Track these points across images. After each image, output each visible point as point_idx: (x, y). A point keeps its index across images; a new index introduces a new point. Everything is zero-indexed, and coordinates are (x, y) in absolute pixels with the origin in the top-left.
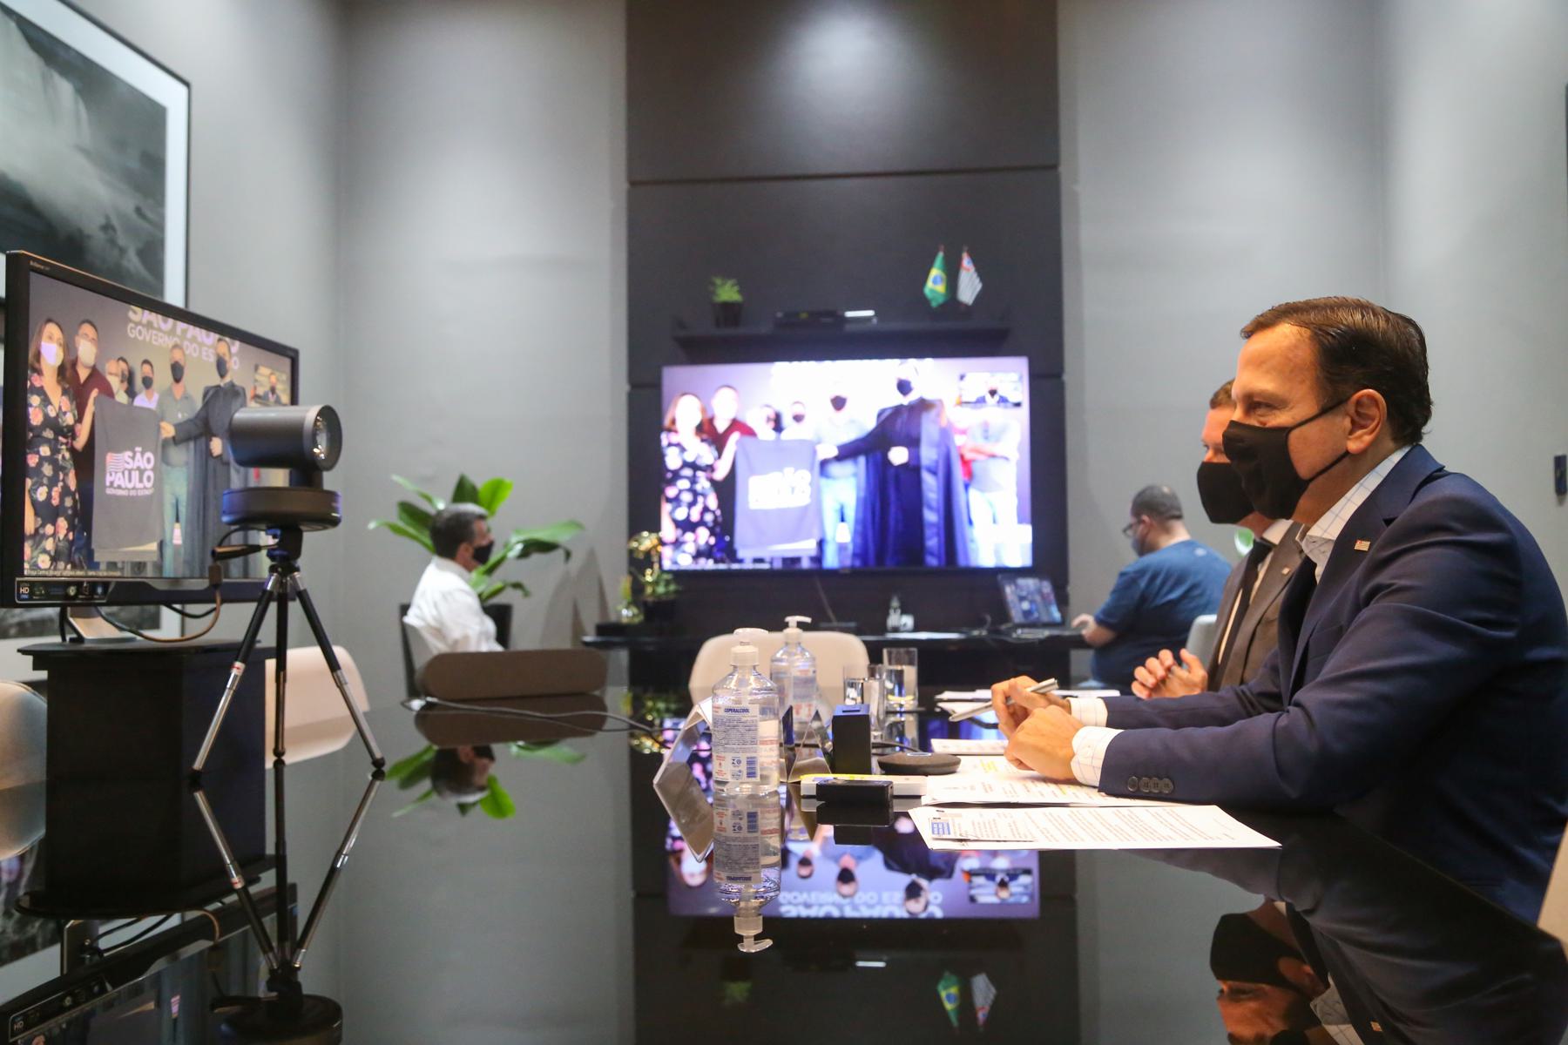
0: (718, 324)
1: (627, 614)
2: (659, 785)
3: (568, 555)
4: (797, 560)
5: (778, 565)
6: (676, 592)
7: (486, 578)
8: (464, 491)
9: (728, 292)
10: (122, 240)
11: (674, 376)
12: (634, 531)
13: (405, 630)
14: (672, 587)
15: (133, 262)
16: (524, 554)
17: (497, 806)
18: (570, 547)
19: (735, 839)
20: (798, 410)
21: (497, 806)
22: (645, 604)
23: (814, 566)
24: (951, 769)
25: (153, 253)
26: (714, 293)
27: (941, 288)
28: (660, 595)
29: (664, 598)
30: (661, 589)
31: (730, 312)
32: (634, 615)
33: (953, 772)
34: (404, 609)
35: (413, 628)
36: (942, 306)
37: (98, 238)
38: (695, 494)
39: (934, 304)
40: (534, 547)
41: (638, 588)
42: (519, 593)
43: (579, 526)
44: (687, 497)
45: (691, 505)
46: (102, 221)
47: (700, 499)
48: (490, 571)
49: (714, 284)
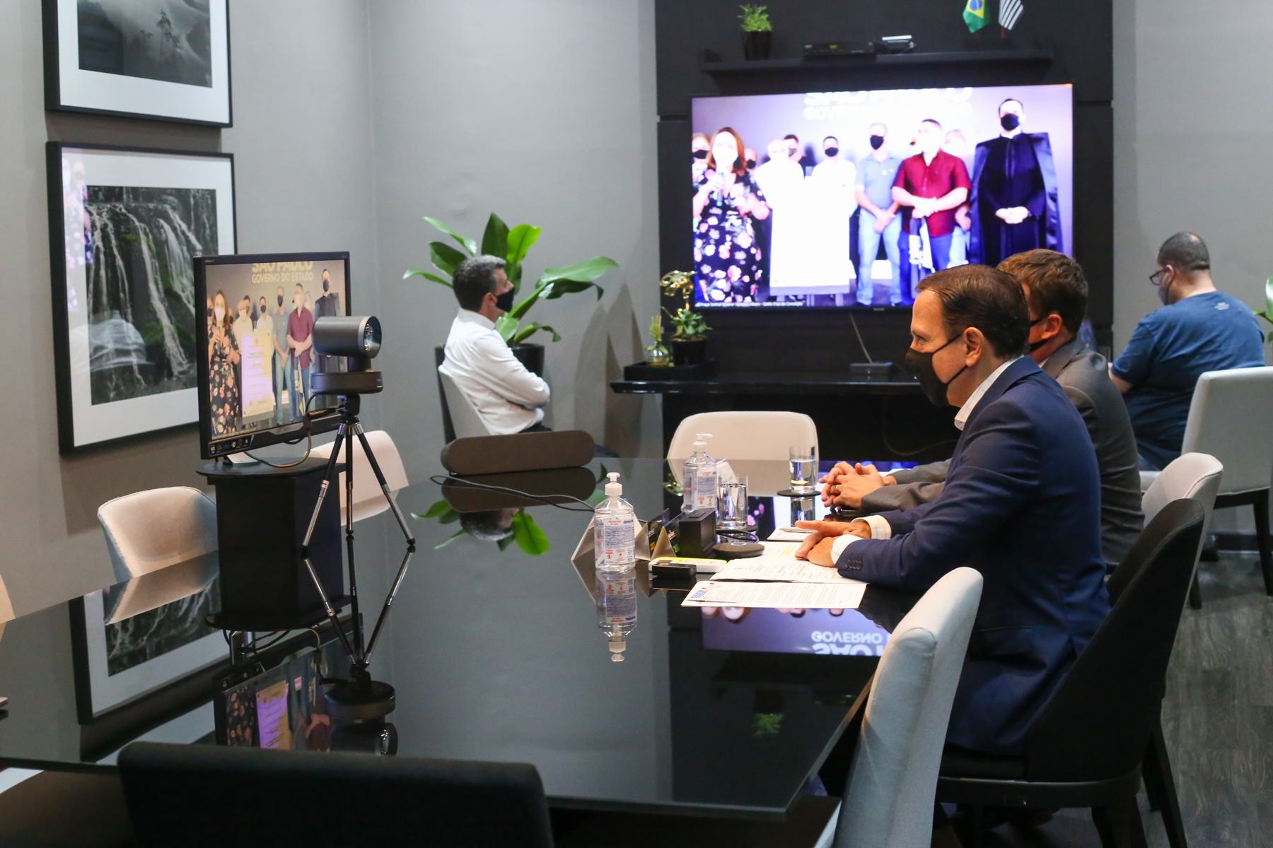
0: (747, 57)
1: (657, 355)
2: (574, 561)
3: (601, 292)
4: (832, 298)
5: (811, 303)
6: (705, 332)
7: (516, 321)
8: (495, 236)
9: (757, 22)
10: (175, 31)
11: (707, 108)
12: (666, 269)
13: (442, 380)
14: (701, 328)
15: (185, 48)
16: (555, 294)
17: (534, 546)
18: (603, 287)
19: (630, 596)
20: (830, 144)
21: (534, 546)
22: (675, 343)
23: (850, 303)
24: (759, 553)
25: (200, 37)
26: (742, 21)
27: (980, 13)
28: (689, 337)
29: (694, 339)
30: (690, 331)
31: (759, 43)
32: (664, 356)
33: (760, 555)
34: (440, 356)
35: (447, 377)
36: (978, 32)
37: (156, 31)
38: (723, 232)
39: (972, 30)
40: (563, 287)
41: (669, 326)
42: (549, 335)
43: (612, 262)
44: (715, 234)
45: (719, 242)
46: (159, 17)
47: (728, 238)
48: (519, 314)
49: (742, 12)
